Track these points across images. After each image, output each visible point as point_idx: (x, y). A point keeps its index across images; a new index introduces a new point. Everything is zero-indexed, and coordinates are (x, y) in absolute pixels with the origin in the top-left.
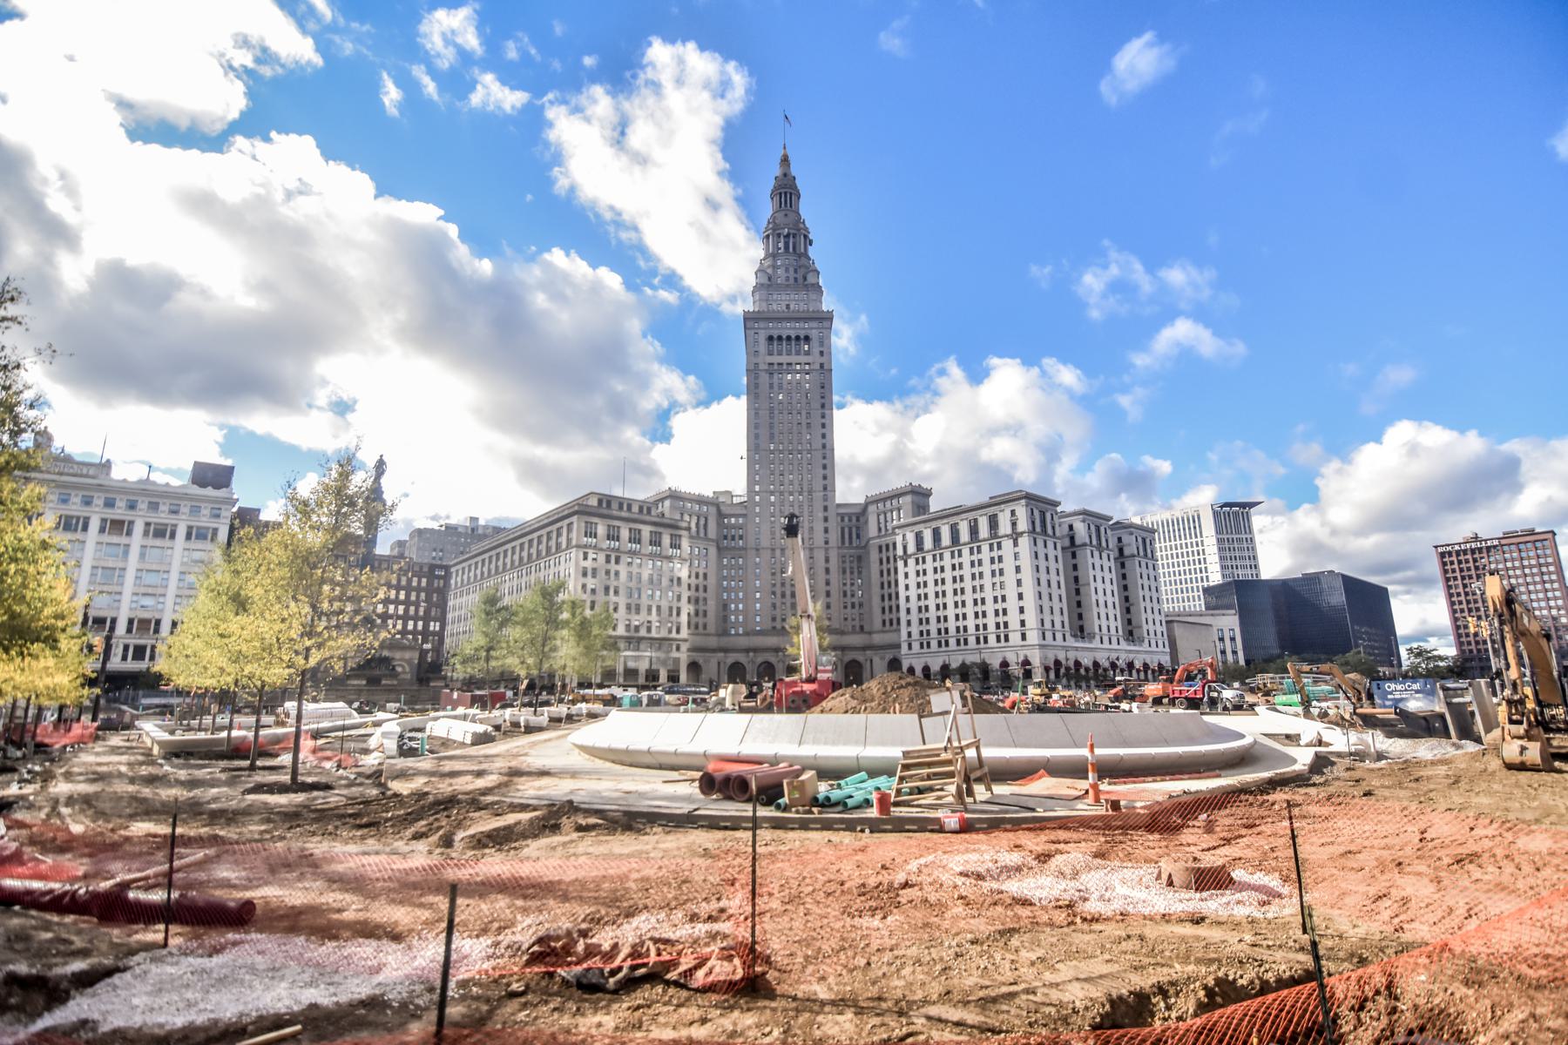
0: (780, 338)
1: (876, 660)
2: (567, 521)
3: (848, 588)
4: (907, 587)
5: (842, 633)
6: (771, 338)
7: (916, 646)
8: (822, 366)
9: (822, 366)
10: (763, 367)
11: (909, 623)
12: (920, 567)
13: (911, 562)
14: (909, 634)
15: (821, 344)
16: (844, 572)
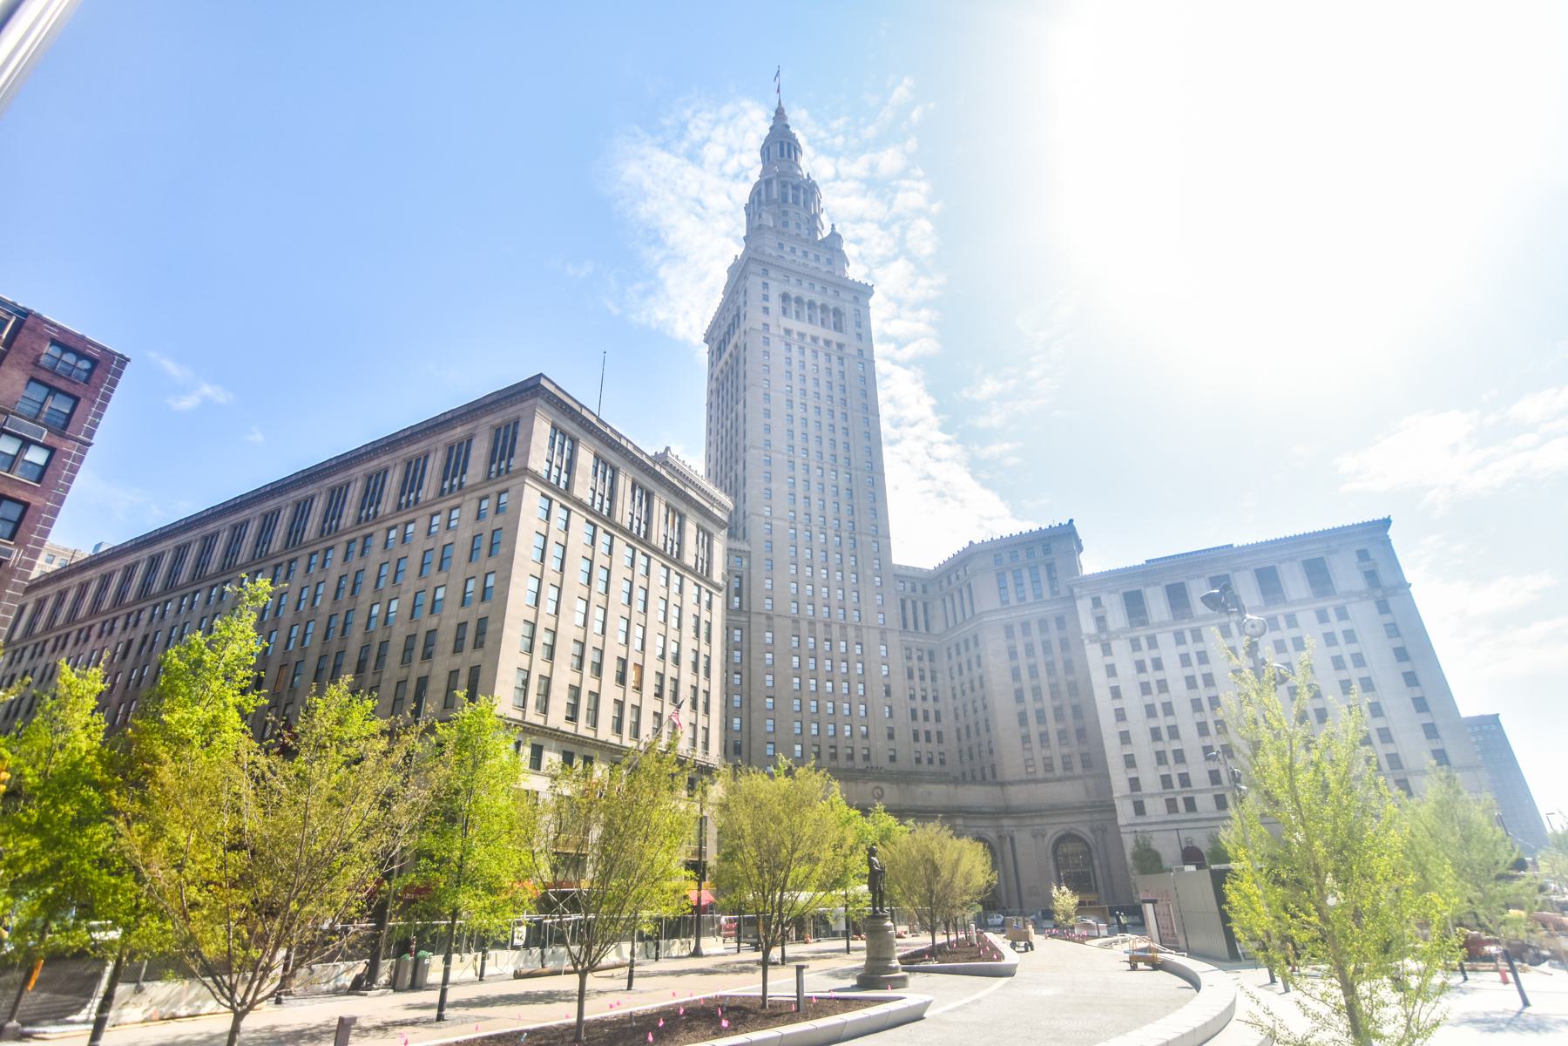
0: (799, 301)
1: (1023, 837)
2: (497, 419)
3: (919, 705)
4: (1116, 693)
5: (956, 781)
6: (785, 297)
7: (1156, 808)
8: (860, 351)
9: (860, 351)
10: (773, 329)
11: (1130, 761)
12: (1147, 655)
13: (1120, 647)
14: (1135, 784)
15: (859, 325)
16: (910, 676)
